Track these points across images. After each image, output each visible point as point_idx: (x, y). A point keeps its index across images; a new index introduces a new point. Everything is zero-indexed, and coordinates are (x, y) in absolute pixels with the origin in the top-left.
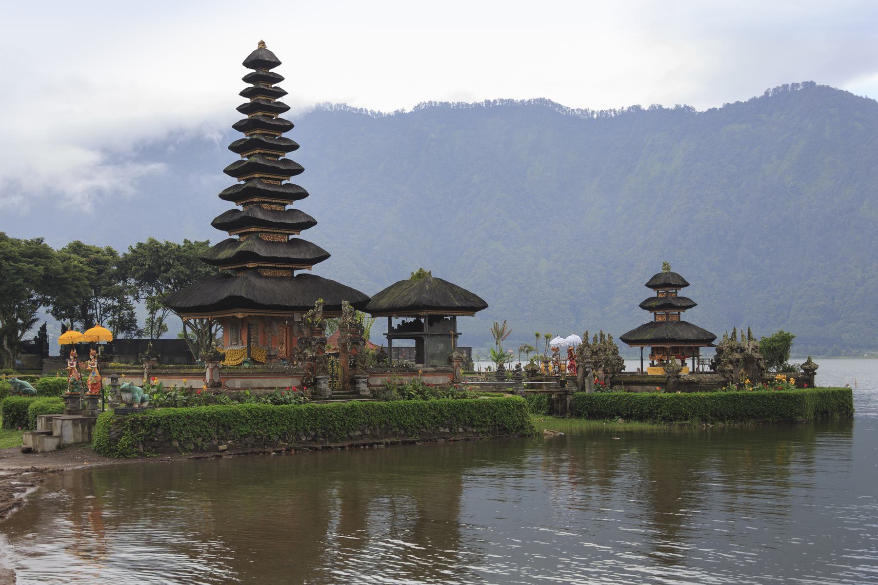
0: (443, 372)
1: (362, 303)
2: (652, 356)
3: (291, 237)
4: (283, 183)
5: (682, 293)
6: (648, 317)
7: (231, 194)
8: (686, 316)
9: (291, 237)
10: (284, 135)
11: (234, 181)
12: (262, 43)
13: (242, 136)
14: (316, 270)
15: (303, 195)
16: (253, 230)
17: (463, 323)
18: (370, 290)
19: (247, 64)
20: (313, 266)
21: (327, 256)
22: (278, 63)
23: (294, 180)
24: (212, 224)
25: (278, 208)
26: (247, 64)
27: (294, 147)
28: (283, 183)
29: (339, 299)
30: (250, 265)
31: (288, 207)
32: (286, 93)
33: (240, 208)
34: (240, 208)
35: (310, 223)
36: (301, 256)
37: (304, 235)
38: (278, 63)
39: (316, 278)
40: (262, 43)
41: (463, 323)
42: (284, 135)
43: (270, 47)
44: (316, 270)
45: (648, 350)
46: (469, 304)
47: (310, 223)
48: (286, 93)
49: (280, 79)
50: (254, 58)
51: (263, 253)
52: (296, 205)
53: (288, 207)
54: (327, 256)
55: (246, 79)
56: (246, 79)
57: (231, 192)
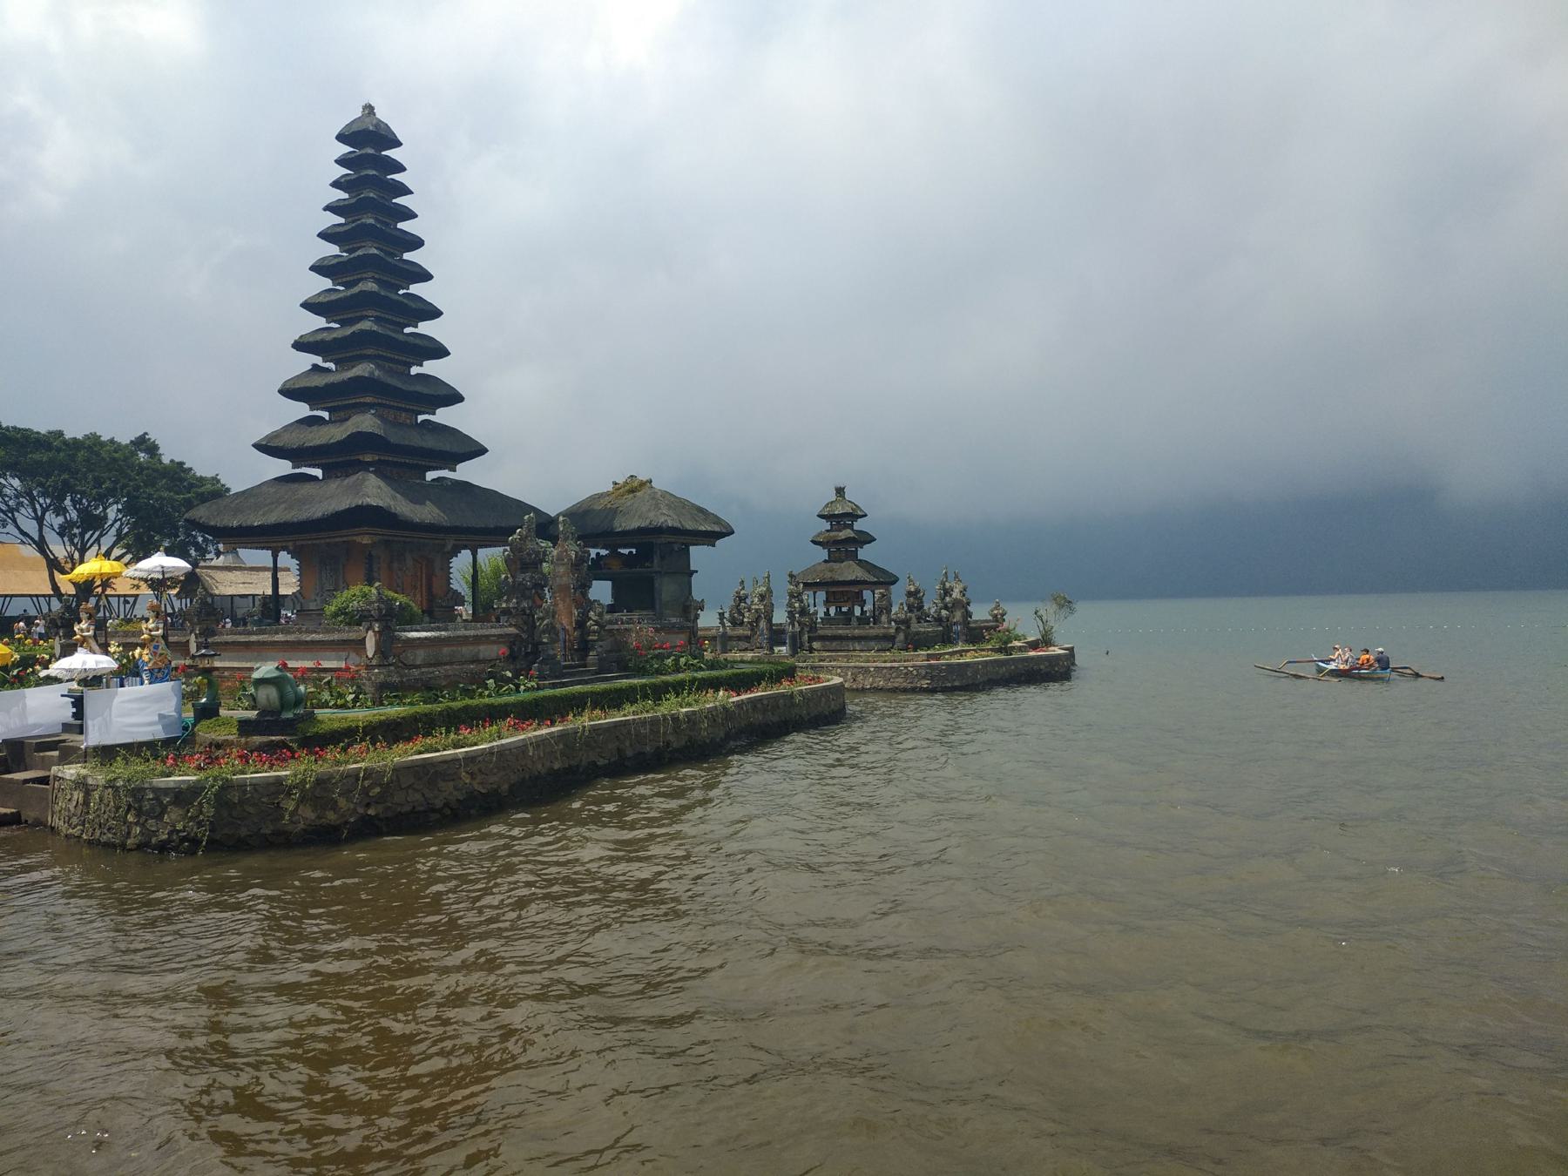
0: (681, 629)
1: (545, 526)
2: (827, 602)
3: (421, 418)
4: (407, 330)
5: (859, 525)
6: (823, 554)
7: (322, 341)
8: (864, 553)
9: (421, 418)
10: (407, 256)
11: (321, 322)
13: (333, 250)
14: (467, 472)
15: (440, 352)
16: (368, 400)
17: (698, 555)
18: (553, 505)
19: (341, 138)
21: (479, 451)
22: (398, 144)
23: (425, 328)
24: (280, 392)
25: (401, 368)
26: (341, 138)
27: (425, 276)
28: (407, 330)
29: (494, 517)
30: (368, 458)
31: (415, 370)
33: (332, 366)
34: (332, 366)
35: (454, 398)
36: (447, 448)
37: (443, 416)
38: (398, 144)
39: (466, 487)
40: (369, 109)
41: (698, 555)
42: (407, 256)
43: (381, 114)
44: (467, 472)
45: (821, 595)
46: (717, 529)
49: (400, 168)
50: (355, 128)
51: (395, 437)
52: (430, 367)
53: (415, 370)
54: (479, 451)
55: (341, 162)
56: (341, 162)
57: (319, 337)
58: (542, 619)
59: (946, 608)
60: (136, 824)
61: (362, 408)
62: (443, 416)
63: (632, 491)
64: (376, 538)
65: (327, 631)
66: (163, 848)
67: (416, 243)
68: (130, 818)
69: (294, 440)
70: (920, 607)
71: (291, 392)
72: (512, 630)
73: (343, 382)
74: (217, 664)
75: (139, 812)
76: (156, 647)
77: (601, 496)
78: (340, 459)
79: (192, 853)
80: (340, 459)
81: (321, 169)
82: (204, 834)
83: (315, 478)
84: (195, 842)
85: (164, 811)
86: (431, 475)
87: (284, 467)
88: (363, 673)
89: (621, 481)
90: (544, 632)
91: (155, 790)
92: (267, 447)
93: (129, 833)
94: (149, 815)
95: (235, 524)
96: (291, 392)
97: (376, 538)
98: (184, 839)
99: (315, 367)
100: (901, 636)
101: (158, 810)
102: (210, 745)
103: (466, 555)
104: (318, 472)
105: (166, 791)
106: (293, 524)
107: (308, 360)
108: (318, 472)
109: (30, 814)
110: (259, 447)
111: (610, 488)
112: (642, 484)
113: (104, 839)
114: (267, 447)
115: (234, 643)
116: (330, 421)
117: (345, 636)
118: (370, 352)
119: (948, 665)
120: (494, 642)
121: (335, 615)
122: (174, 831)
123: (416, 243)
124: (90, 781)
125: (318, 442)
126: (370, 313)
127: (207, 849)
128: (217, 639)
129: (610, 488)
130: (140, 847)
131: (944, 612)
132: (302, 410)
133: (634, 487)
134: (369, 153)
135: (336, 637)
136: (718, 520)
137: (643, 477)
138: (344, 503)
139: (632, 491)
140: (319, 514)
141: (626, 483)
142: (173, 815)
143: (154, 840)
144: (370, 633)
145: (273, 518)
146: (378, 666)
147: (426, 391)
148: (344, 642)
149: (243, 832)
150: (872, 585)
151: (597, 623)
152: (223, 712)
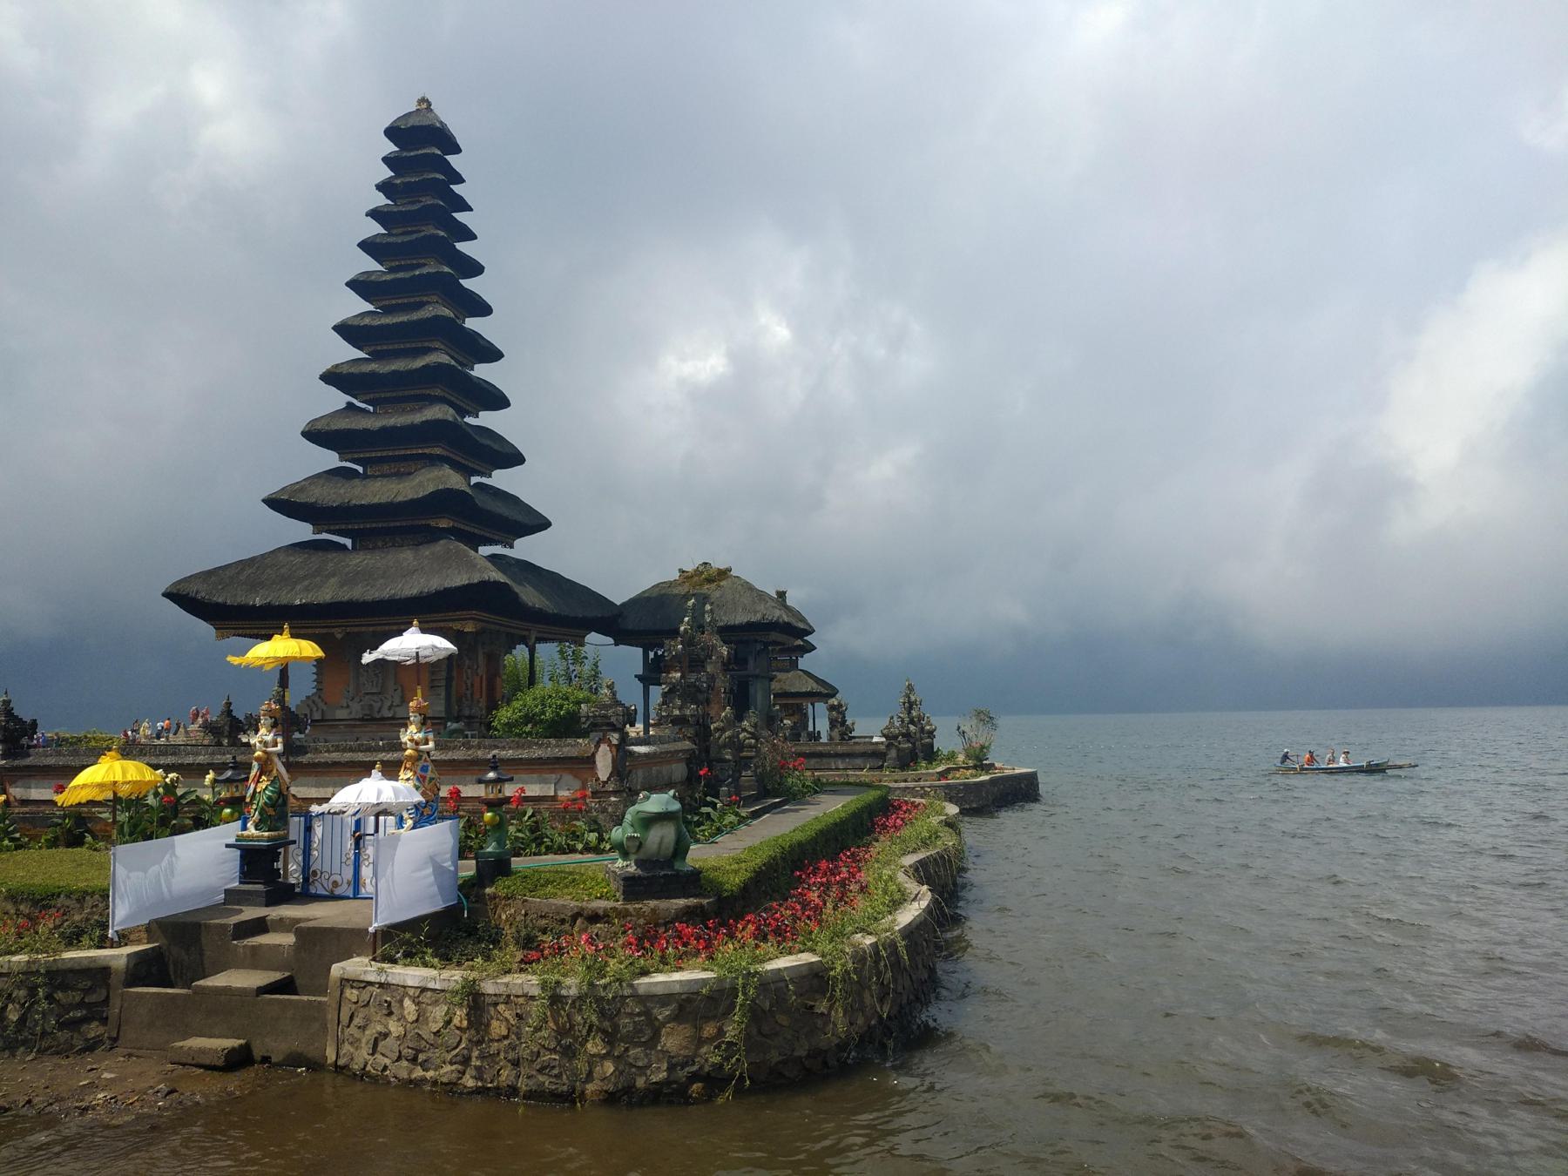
3: (475, 480)
11: (351, 353)
14: (526, 549)
16: (438, 451)
19: (392, 133)
20: (517, 542)
21: (543, 524)
22: (457, 150)
26: (392, 133)
31: (470, 420)
35: (513, 458)
37: (501, 479)
38: (457, 150)
39: (527, 570)
47: (513, 458)
52: (486, 419)
53: (470, 420)
54: (543, 524)
58: (723, 730)
59: (912, 722)
60: (603, 1057)
61: (433, 461)
62: (501, 479)
63: (710, 580)
64: (480, 625)
65: (518, 746)
66: (659, 1096)
67: (475, 269)
68: (594, 1046)
70: (843, 722)
71: (317, 435)
72: (687, 745)
73: (412, 427)
74: (509, 790)
75: (610, 1038)
76: (424, 769)
77: (671, 584)
78: (376, 527)
79: (708, 1097)
80: (376, 527)
81: (364, 169)
82: (740, 1064)
83: (344, 547)
84: (715, 1081)
85: (656, 1037)
86: (485, 550)
87: (303, 531)
88: (593, 803)
89: (690, 568)
90: (725, 746)
91: (637, 997)
92: (280, 504)
93: (590, 1074)
94: (631, 1040)
95: (258, 602)
96: (317, 435)
97: (480, 625)
98: (694, 1077)
99: (350, 406)
100: (893, 753)
101: (649, 1032)
102: (575, 917)
103: (521, 652)
104: (348, 542)
105: (665, 999)
106: (365, 604)
107: (337, 400)
108: (348, 542)
109: (276, 1046)
110: (273, 503)
111: (676, 576)
112: (724, 574)
113: (523, 1085)
114: (280, 504)
115: (336, 764)
116: (365, 476)
117: (557, 752)
118: (438, 392)
119: (965, 785)
120: (680, 760)
121: (509, 726)
122: (671, 1068)
123: (475, 269)
124: (489, 988)
125: (411, 495)
126: (437, 345)
127: (739, 1092)
128: (304, 759)
129: (676, 576)
130: (611, 1099)
131: (912, 728)
132: (330, 459)
133: (711, 577)
134: (421, 157)
135: (537, 753)
136: (803, 620)
137: (719, 563)
138: (459, 579)
139: (710, 580)
140: (415, 592)
141: (697, 572)
142: (673, 1041)
143: (640, 1082)
144: (604, 748)
145: (326, 594)
146: (615, 793)
147: (496, 447)
148: (558, 760)
149: (774, 1057)
150: (812, 696)
151: (753, 736)
152: (517, 863)
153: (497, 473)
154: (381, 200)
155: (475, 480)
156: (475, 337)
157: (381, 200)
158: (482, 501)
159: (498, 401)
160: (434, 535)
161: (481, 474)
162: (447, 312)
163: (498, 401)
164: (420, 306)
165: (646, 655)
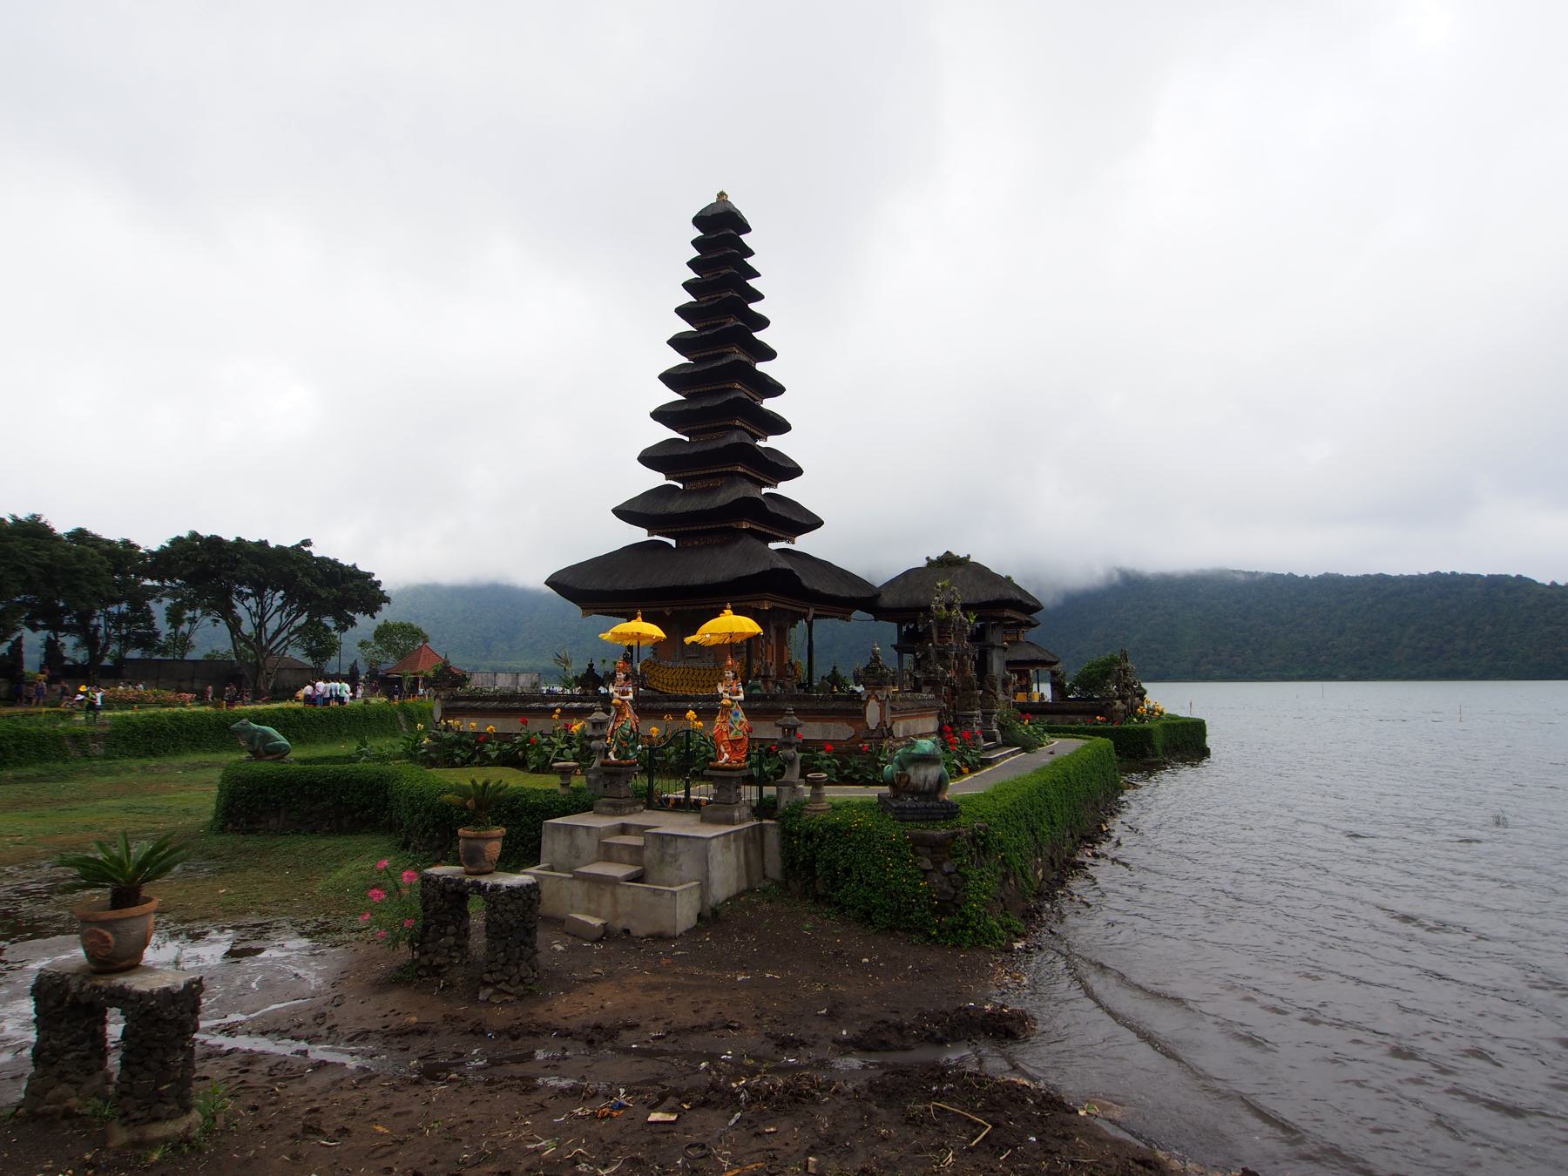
3: (765, 490)
12: (722, 194)
14: (804, 543)
16: (740, 469)
19: (699, 221)
20: (798, 539)
21: (813, 523)
22: (747, 229)
26: (699, 221)
31: (760, 443)
32: (758, 275)
35: (793, 471)
37: (785, 489)
38: (747, 229)
40: (722, 194)
44: (804, 543)
47: (793, 471)
48: (758, 275)
50: (709, 214)
52: (773, 442)
53: (760, 443)
54: (816, 523)
62: (785, 489)
67: (763, 323)
69: (660, 509)
86: (773, 546)
89: (934, 558)
96: (650, 458)
103: (802, 623)
108: (673, 542)
123: (763, 323)
132: (657, 479)
134: (721, 238)
153: (782, 485)
154: (691, 275)
155: (765, 490)
156: (764, 376)
157: (691, 275)
158: (772, 508)
159: (781, 426)
160: (737, 534)
161: (770, 486)
162: (744, 358)
163: (781, 426)
164: (723, 355)
165: (900, 629)
